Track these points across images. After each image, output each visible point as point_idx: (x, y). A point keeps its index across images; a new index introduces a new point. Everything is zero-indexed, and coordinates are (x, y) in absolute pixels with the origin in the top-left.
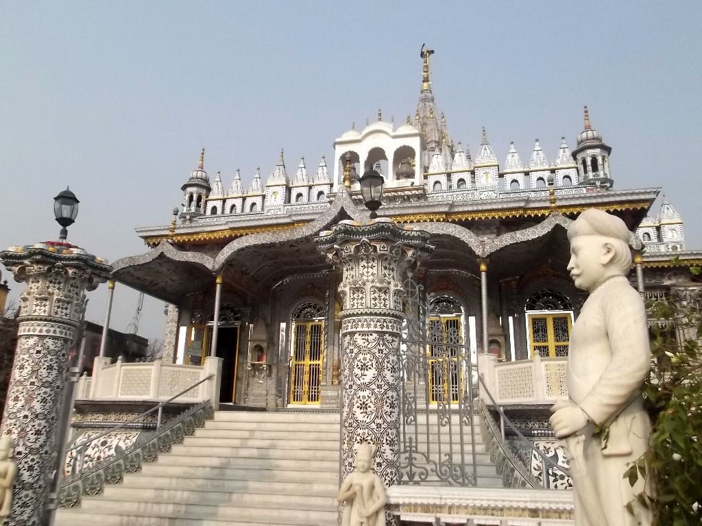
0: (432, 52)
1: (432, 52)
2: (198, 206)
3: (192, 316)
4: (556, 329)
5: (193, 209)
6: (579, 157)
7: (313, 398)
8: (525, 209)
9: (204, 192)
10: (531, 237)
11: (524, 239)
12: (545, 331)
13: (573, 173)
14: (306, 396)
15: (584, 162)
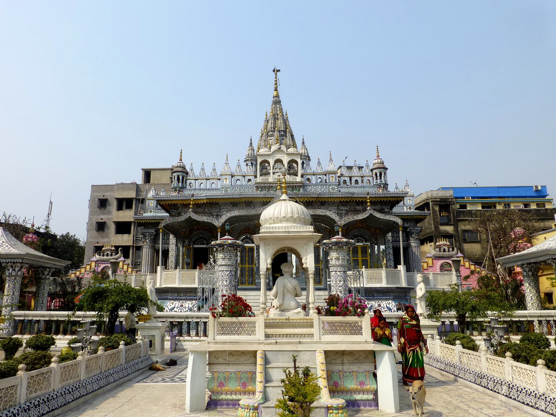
0: (279, 71)
1: (279, 71)
2: (183, 182)
3: (184, 242)
4: (362, 253)
5: (180, 185)
6: (374, 171)
7: (252, 284)
8: (351, 197)
9: (185, 174)
10: (361, 218)
11: (358, 218)
12: (357, 253)
13: (371, 179)
14: (247, 282)
15: (376, 174)
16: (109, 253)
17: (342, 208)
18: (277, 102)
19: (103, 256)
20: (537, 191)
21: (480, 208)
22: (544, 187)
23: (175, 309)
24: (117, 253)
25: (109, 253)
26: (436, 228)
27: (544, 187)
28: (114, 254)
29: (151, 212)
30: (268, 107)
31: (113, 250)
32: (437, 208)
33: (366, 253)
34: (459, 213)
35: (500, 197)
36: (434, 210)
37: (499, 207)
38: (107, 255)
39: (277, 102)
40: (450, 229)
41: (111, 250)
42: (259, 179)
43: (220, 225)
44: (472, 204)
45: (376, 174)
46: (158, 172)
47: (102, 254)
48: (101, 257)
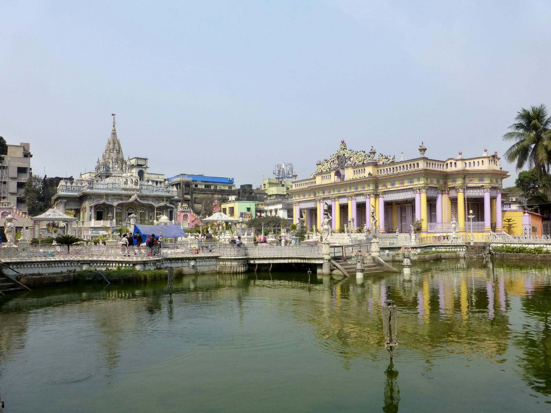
18: (114, 134)
20: (230, 180)
21: (204, 187)
22: (233, 179)
26: (183, 196)
27: (233, 179)
30: (109, 136)
32: (184, 186)
34: (194, 189)
35: (213, 182)
36: (183, 187)
37: (212, 188)
39: (114, 134)
40: (189, 197)
44: (201, 184)
46: (13, 148)
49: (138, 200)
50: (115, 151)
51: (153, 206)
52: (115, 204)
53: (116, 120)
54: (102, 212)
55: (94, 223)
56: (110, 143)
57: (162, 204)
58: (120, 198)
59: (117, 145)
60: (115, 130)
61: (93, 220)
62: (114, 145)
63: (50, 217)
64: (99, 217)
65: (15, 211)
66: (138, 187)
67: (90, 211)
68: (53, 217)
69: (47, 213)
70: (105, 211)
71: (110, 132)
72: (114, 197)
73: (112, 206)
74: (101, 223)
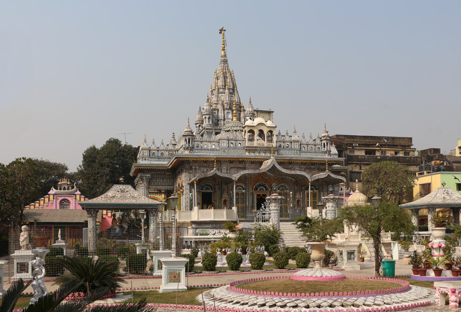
6: (323, 142)
15: (324, 144)
16: (66, 187)
17: (302, 166)
19: (60, 189)
23: (216, 234)
24: (73, 187)
25: (66, 187)
28: (70, 188)
29: (145, 159)
31: (69, 184)
33: (315, 197)
37: (378, 154)
38: (64, 189)
41: (68, 184)
42: (247, 144)
43: (236, 179)
45: (324, 144)
47: (59, 188)
48: (59, 190)
49: (278, 167)
50: (227, 91)
51: (304, 178)
52: (236, 176)
53: (226, 38)
54: (211, 193)
55: (197, 214)
56: (217, 78)
57: (322, 175)
58: (241, 166)
59: (228, 80)
60: (225, 56)
61: (196, 208)
62: (225, 81)
63: (114, 201)
64: (206, 201)
65: (78, 197)
66: (274, 145)
67: (191, 192)
68: (121, 202)
69: (110, 193)
70: (215, 192)
71: (219, 59)
72: (232, 165)
73: (229, 181)
74: (210, 215)
